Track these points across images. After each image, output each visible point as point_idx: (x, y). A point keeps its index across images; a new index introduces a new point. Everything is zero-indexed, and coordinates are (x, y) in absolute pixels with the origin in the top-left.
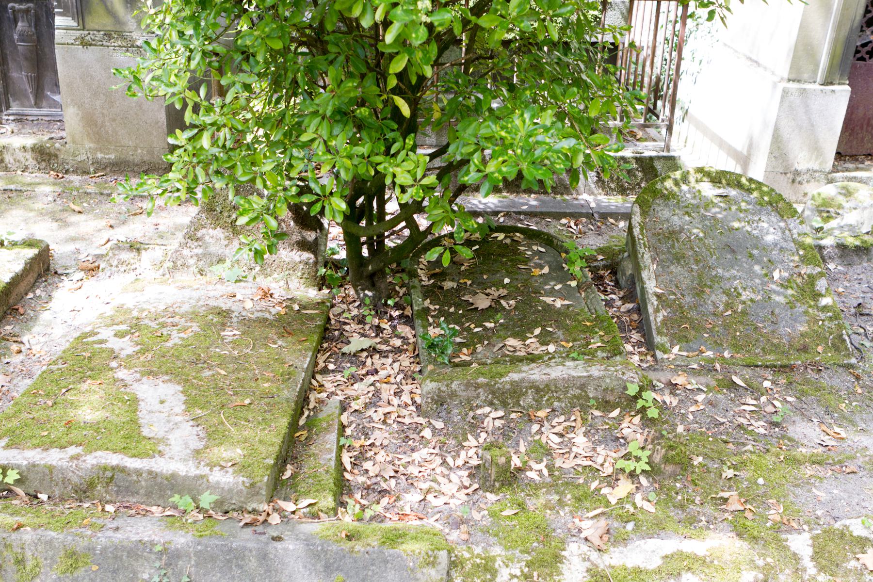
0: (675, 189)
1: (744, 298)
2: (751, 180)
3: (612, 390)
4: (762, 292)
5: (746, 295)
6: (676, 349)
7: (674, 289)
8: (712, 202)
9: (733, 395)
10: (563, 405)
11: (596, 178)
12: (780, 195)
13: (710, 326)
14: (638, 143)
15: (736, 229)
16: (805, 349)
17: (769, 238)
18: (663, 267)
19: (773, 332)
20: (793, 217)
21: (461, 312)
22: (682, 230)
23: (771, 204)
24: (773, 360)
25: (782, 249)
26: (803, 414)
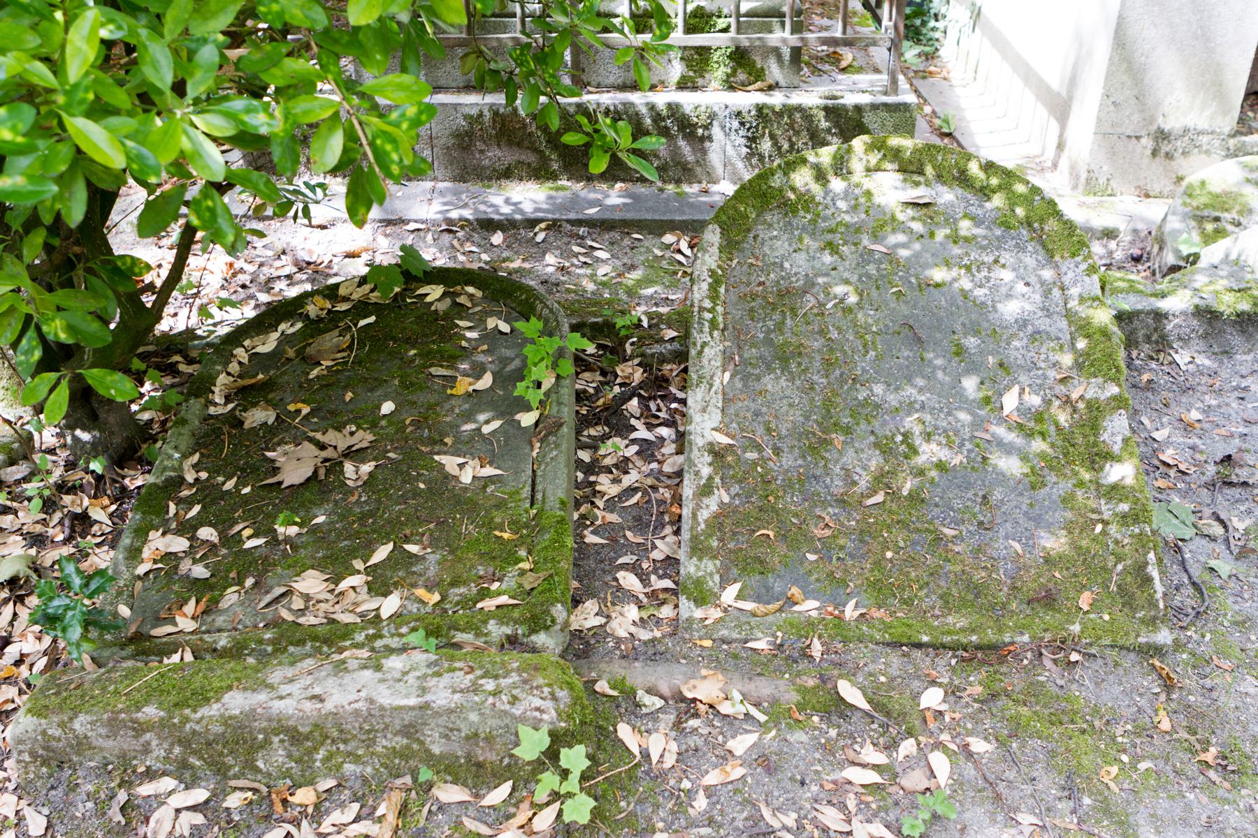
0: (816, 188)
1: (920, 460)
2: (989, 167)
3: (489, 739)
4: (968, 446)
5: (930, 452)
6: (729, 595)
7: (760, 435)
8: (893, 218)
9: (833, 733)
10: (369, 769)
11: (745, 150)
12: (1052, 203)
13: (827, 532)
14: (840, 77)
15: (937, 285)
16: (1048, 600)
17: (1010, 309)
18: (745, 379)
19: (978, 551)
20: (1073, 255)
21: (247, 490)
22: (810, 284)
23: (1030, 225)
24: (962, 630)
25: (1036, 337)
26: (998, 797)
